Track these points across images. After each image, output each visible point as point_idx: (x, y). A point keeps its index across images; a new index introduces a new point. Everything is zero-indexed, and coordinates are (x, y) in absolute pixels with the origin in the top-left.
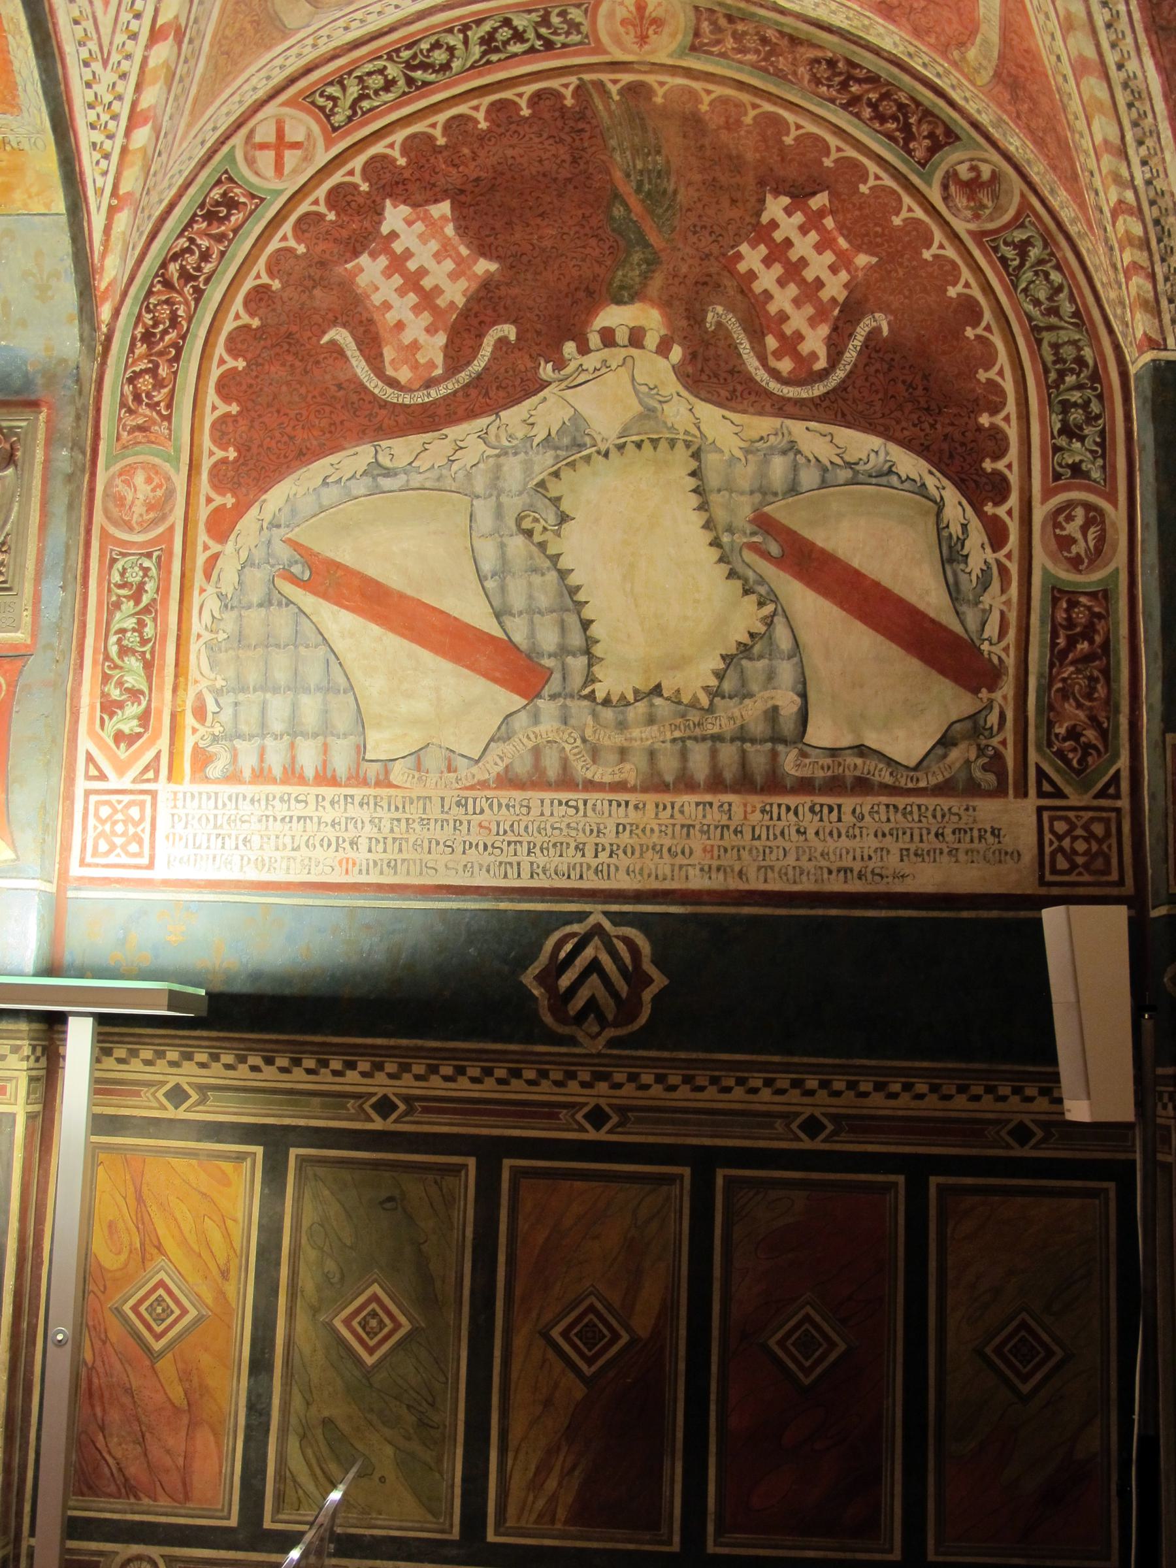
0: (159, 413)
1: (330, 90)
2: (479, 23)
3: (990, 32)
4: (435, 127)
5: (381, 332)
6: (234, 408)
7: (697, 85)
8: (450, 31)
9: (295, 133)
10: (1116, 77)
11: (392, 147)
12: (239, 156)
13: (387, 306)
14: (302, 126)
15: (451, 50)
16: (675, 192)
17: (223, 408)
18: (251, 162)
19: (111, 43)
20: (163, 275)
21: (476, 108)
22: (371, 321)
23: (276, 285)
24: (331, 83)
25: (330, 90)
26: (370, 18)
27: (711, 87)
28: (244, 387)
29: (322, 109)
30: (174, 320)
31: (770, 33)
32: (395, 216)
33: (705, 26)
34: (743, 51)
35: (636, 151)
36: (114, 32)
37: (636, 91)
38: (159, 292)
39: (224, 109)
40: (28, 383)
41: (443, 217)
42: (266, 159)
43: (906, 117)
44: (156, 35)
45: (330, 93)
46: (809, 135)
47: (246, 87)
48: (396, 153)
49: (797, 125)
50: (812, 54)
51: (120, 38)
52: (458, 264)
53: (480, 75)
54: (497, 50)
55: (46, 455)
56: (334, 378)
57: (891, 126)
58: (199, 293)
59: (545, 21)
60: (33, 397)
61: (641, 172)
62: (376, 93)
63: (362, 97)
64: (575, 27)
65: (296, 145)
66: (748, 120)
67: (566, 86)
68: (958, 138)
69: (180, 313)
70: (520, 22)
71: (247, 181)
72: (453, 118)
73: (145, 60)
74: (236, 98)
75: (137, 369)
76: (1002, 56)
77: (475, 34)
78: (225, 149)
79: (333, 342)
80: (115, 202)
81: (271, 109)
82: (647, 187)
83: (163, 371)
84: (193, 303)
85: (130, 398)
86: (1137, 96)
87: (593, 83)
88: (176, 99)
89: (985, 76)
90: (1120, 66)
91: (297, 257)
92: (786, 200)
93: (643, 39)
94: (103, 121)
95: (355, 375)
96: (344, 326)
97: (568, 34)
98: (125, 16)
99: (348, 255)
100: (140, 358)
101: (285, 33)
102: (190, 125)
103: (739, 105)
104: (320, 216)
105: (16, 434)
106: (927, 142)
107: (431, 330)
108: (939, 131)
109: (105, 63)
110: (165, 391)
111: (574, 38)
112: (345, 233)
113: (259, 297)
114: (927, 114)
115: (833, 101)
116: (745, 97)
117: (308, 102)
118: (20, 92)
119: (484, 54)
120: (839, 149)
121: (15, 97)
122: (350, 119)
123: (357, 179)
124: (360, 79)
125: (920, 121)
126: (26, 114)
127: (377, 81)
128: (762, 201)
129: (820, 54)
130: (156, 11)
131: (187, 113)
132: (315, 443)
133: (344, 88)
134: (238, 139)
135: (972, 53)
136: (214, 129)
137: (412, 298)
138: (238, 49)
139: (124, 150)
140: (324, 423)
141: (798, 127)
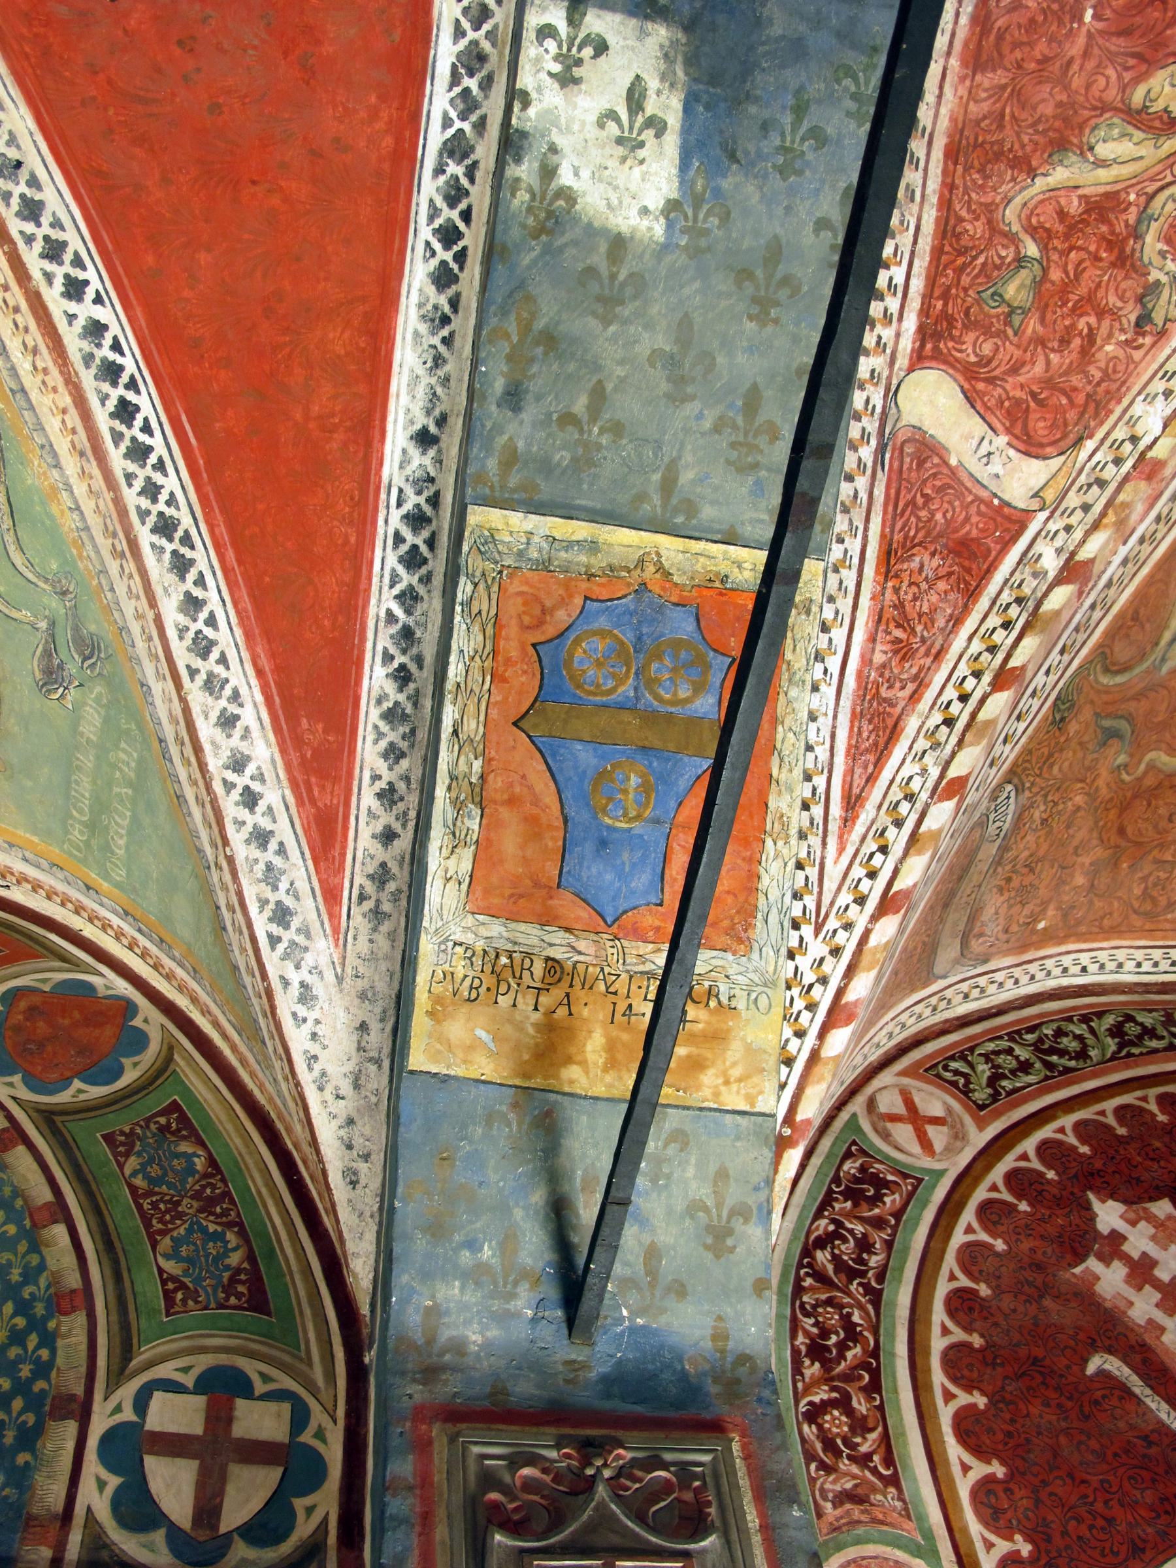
0: (874, 1471)
1: (954, 1065)
6: (998, 1470)
14: (933, 1101)
17: (980, 1470)
18: (886, 1136)
19: (832, 903)
20: (810, 1265)
23: (984, 1290)
24: (952, 1058)
28: (1000, 1436)
30: (852, 1333)
36: (839, 889)
38: (811, 1288)
40: (690, 1389)
44: (887, 904)
51: (845, 898)
53: (1128, 1067)
55: (762, 1515)
56: (1132, 1427)
58: (876, 1297)
60: (706, 1415)
69: (856, 1318)
71: (888, 1157)
73: (866, 934)
75: (816, 1399)
78: (844, 1116)
79: (1102, 1374)
80: (787, 1132)
81: (886, 1078)
83: (860, 1405)
84: (870, 1307)
85: (819, 1446)
94: (795, 1010)
95: (1160, 1422)
96: (1111, 1353)
98: (858, 872)
99: (1069, 1257)
100: (815, 1383)
105: (695, 1476)
109: (818, 929)
110: (874, 1436)
112: (1052, 1231)
113: (962, 1305)
118: (759, 923)
121: (748, 927)
126: (755, 955)
132: (1150, 1530)
134: (857, 1105)
139: (814, 1057)
140: (1149, 1497)
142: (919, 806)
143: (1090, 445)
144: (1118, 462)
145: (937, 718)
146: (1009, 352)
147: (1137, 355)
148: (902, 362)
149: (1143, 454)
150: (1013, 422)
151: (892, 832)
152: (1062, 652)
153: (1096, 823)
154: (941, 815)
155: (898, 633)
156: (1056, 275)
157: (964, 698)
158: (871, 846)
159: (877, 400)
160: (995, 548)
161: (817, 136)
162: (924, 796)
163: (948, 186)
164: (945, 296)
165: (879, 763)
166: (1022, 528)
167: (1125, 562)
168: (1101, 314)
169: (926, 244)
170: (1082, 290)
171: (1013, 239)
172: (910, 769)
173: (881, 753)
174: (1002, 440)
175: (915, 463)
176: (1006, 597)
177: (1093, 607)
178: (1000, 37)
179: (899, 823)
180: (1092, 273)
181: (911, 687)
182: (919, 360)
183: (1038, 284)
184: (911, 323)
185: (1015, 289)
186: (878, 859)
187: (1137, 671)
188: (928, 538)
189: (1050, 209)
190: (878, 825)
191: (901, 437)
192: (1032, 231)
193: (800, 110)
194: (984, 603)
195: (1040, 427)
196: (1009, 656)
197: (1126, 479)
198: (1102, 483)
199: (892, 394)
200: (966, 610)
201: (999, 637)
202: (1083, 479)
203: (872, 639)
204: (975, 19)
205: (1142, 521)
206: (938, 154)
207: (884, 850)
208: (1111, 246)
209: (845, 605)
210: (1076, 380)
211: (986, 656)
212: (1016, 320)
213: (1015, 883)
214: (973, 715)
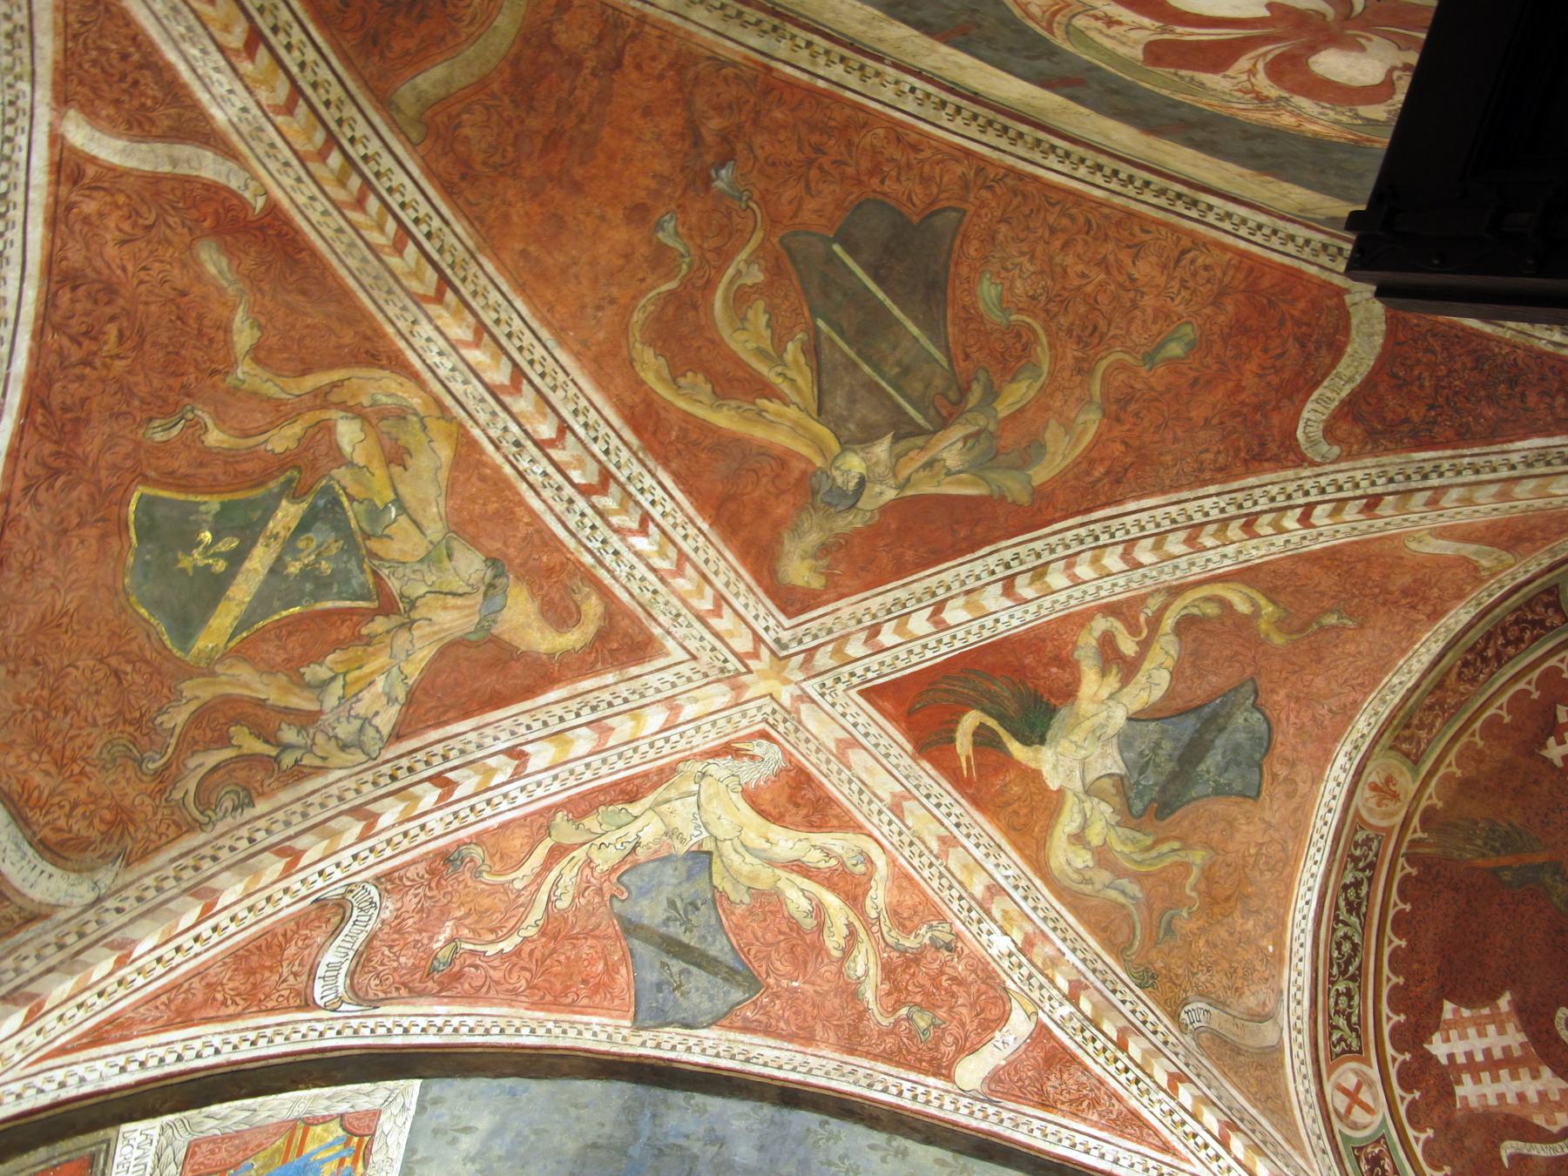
1: (1334, 1038)
2: (1337, 908)
3: (1469, 550)
4: (1390, 979)
5: (1518, 1114)
7: (1442, 771)
8: (1334, 930)
9: (1351, 1082)
10: (1521, 470)
11: (1391, 1019)
12: (1347, 1131)
13: (1501, 1097)
14: (1347, 1075)
15: (1346, 937)
16: (1510, 824)
18: (1355, 1126)
21: (1391, 942)
22: (1508, 1117)
25: (1334, 1038)
26: (1300, 982)
27: (1447, 761)
29: (1344, 1052)
31: (1427, 702)
32: (1439, 1048)
33: (1405, 746)
34: (1432, 725)
35: (1469, 840)
37: (1426, 820)
39: (1309, 1121)
41: (1455, 1012)
42: (1358, 1114)
43: (1525, 621)
44: (1224, 1142)
45: (1337, 1040)
46: (1509, 701)
47: (1302, 1097)
48: (1395, 1018)
49: (1499, 708)
50: (1453, 676)
52: (1494, 1022)
53: (1370, 926)
54: (1360, 904)
57: (1527, 635)
59: (1356, 860)
61: (1486, 844)
62: (1350, 1007)
63: (1348, 1020)
64: (1368, 840)
65: (1359, 1087)
66: (1481, 744)
67: (1403, 868)
68: (1556, 586)
70: (1349, 879)
71: (1366, 1138)
72: (1390, 962)
74: (1305, 1108)
76: (1491, 544)
77: (1343, 915)
78: (1338, 1138)
81: (1328, 1088)
82: (1497, 845)
86: (1543, 456)
87: (1409, 847)
88: (1276, 1154)
89: (1508, 557)
90: (1513, 467)
91: (1434, 1139)
92: (1551, 741)
93: (1395, 796)
96: (1502, 1140)
97: (1370, 849)
98: (1202, 1154)
101: (1278, 1049)
102: (1304, 1155)
103: (1468, 746)
104: (1413, 1103)
106: (1550, 612)
107: (1535, 1075)
108: (1546, 598)
111: (1375, 845)
112: (1434, 1093)
114: (1529, 604)
115: (1492, 673)
116: (1464, 739)
117: (1336, 1058)
119: (1358, 916)
120: (1529, 683)
122: (1358, 1037)
123: (1400, 1058)
124: (1337, 1012)
125: (1533, 612)
127: (1343, 999)
128: (1545, 759)
129: (1455, 670)
130: (1209, 1132)
131: (1292, 1152)
133: (1337, 1028)
134: (1337, 1125)
135: (1485, 563)
136: (1319, 1137)
137: (1504, 1073)
138: (1270, 1089)
141: (1500, 708)
142: (1177, 1108)
143: (1009, 983)
144: (1020, 966)
145: (1134, 1088)
146: (953, 1027)
147: (966, 951)
148: (949, 1086)
149: (1020, 950)
150: (989, 1027)
151: (1187, 1128)
152: (1114, 992)
153: (1218, 922)
154: (1185, 1094)
155: (1085, 1104)
156: (918, 999)
157: (1127, 1070)
158: (1191, 1142)
159: (966, 1101)
160: (1053, 1043)
161: (842, 1158)
162: (1173, 1104)
163: (867, 1055)
164: (921, 1061)
165: (1149, 1126)
166: (1045, 1027)
167: (1074, 950)
168: (942, 973)
169: (893, 1070)
170: (928, 983)
171: (897, 1022)
172: (1156, 1110)
173: (1146, 1125)
174: (997, 1034)
175: (1001, 1085)
176: (1079, 1039)
177: (1094, 971)
178: (800, 1028)
179: (1183, 1123)
180: (922, 979)
181: (1114, 1101)
182: (949, 1078)
183: (921, 1007)
184: (931, 1081)
185: (922, 1021)
186: (1199, 1140)
187: (1136, 918)
188: (1040, 1081)
189: (885, 1000)
190: (1181, 1135)
191: (986, 1090)
192: (895, 1010)
193: (830, 1163)
194: (1079, 1052)
195: (995, 1012)
196: (1110, 1040)
197: (1030, 961)
198: (1030, 976)
199: (963, 1093)
200: (1081, 1064)
201: (1099, 1045)
202: (1026, 988)
203: (1085, 1120)
204: (791, 1041)
205: (1054, 944)
206: (851, 1059)
207: (1195, 1136)
208: (908, 967)
209: (1064, 1133)
210: (973, 989)
211: (1108, 1054)
212: (938, 1022)
213: (1239, 984)
214: (1137, 1065)
